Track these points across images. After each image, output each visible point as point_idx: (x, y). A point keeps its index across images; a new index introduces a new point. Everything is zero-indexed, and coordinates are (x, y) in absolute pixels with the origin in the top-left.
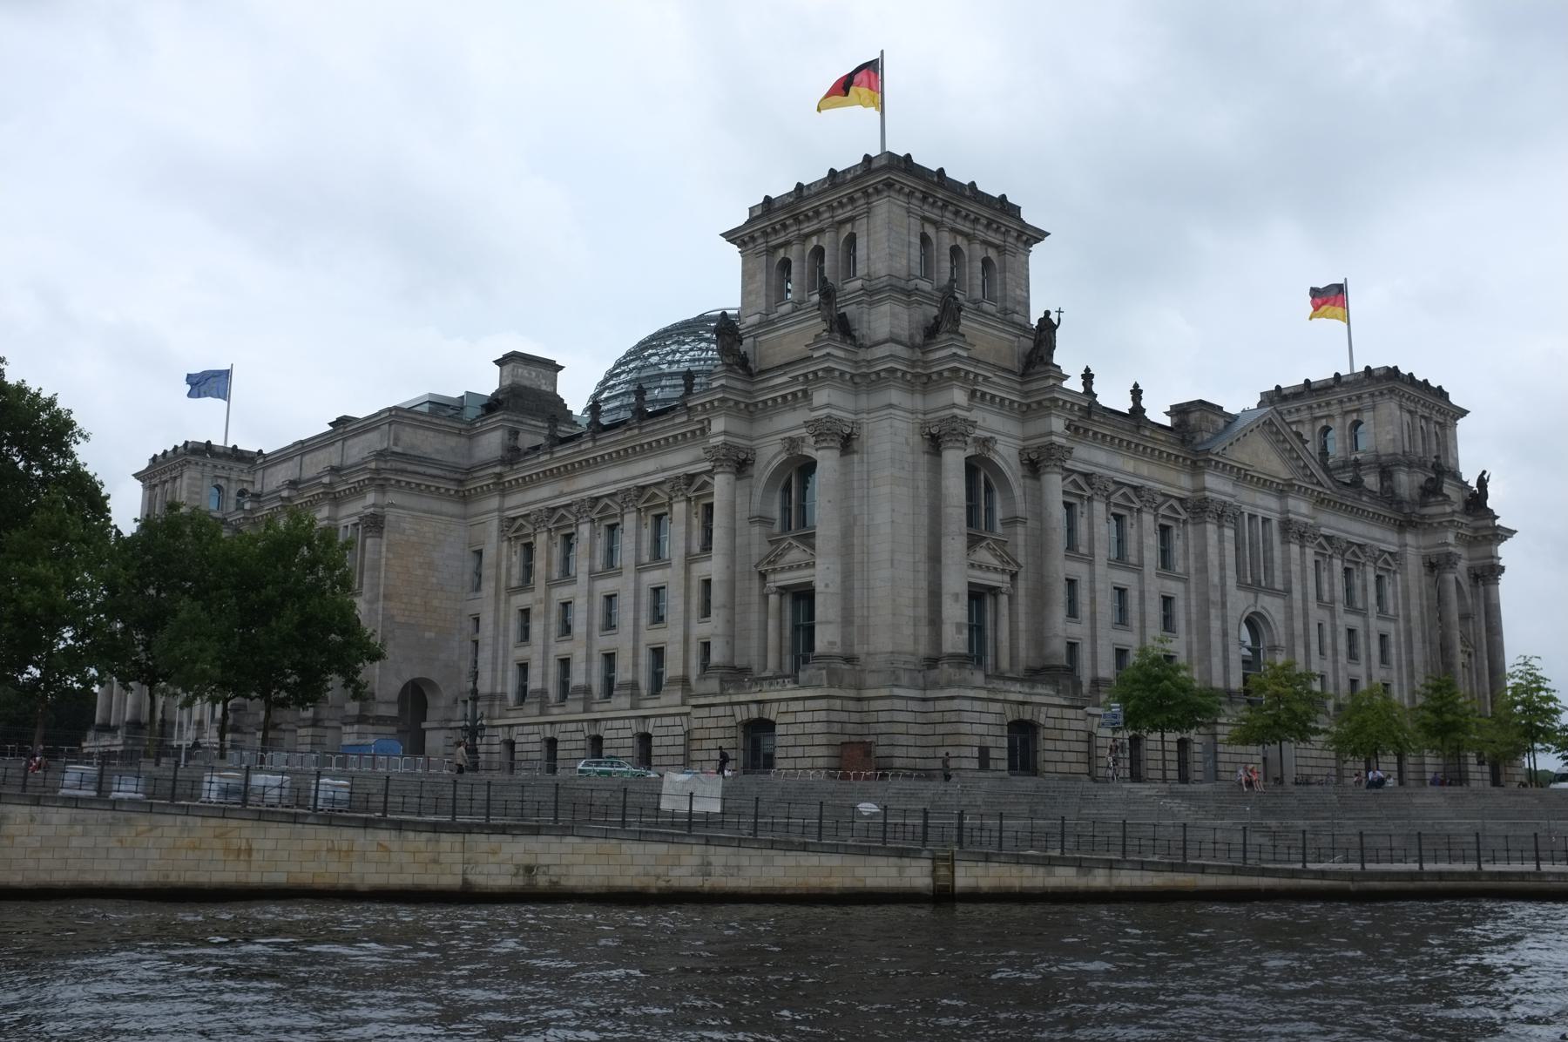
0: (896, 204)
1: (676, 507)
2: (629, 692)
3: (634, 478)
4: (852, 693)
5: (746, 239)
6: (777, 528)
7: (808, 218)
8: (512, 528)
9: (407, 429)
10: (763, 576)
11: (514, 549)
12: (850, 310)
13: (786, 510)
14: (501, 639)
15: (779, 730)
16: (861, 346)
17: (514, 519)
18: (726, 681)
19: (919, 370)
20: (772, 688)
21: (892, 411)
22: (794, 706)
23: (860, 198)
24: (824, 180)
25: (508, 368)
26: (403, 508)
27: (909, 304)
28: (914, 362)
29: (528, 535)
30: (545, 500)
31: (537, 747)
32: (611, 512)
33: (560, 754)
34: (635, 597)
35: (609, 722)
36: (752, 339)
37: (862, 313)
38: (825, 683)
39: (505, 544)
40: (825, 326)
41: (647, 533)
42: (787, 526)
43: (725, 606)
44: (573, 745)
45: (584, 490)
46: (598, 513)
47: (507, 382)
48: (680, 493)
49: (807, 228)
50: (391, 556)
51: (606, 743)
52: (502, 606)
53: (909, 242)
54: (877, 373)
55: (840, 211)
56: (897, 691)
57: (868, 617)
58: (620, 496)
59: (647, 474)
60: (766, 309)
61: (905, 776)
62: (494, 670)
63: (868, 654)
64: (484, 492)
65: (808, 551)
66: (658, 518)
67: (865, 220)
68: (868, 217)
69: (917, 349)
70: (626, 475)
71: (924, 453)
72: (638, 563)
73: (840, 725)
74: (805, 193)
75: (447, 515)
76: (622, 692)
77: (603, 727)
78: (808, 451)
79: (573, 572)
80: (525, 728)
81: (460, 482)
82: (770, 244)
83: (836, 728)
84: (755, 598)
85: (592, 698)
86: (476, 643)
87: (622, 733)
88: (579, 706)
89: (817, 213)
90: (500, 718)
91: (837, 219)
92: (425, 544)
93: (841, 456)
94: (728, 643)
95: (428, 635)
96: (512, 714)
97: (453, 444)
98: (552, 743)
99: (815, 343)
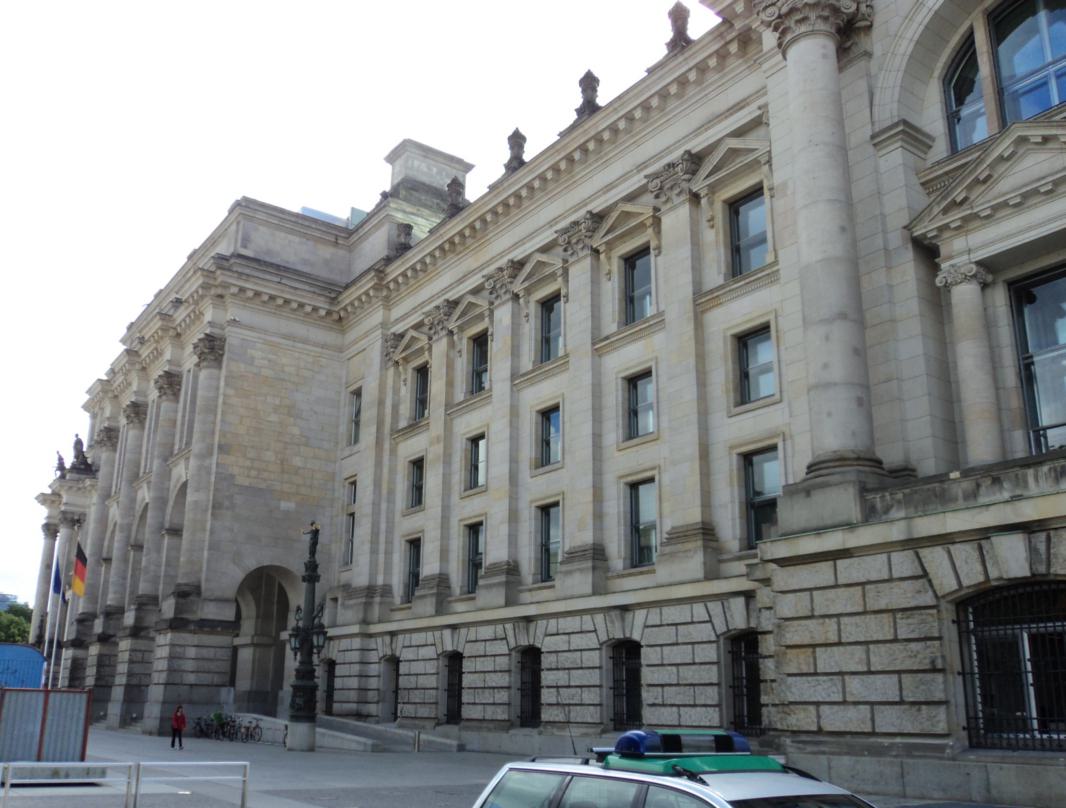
1: (667, 221)
2: (589, 564)
9: (261, 228)
10: (928, 252)
11: (403, 377)
14: (384, 506)
17: (402, 336)
26: (251, 328)
31: (431, 667)
33: (467, 680)
35: (553, 622)
39: (391, 371)
43: (843, 316)
44: (488, 664)
45: (501, 255)
47: (396, 181)
50: (231, 392)
51: (547, 661)
62: (374, 551)
64: (364, 301)
75: (316, 344)
76: (576, 566)
77: (540, 631)
79: (487, 385)
81: (333, 301)
85: (520, 583)
86: (352, 515)
87: (578, 641)
90: (380, 621)
92: (283, 380)
95: (284, 505)
96: (398, 615)
97: (328, 256)
98: (455, 659)
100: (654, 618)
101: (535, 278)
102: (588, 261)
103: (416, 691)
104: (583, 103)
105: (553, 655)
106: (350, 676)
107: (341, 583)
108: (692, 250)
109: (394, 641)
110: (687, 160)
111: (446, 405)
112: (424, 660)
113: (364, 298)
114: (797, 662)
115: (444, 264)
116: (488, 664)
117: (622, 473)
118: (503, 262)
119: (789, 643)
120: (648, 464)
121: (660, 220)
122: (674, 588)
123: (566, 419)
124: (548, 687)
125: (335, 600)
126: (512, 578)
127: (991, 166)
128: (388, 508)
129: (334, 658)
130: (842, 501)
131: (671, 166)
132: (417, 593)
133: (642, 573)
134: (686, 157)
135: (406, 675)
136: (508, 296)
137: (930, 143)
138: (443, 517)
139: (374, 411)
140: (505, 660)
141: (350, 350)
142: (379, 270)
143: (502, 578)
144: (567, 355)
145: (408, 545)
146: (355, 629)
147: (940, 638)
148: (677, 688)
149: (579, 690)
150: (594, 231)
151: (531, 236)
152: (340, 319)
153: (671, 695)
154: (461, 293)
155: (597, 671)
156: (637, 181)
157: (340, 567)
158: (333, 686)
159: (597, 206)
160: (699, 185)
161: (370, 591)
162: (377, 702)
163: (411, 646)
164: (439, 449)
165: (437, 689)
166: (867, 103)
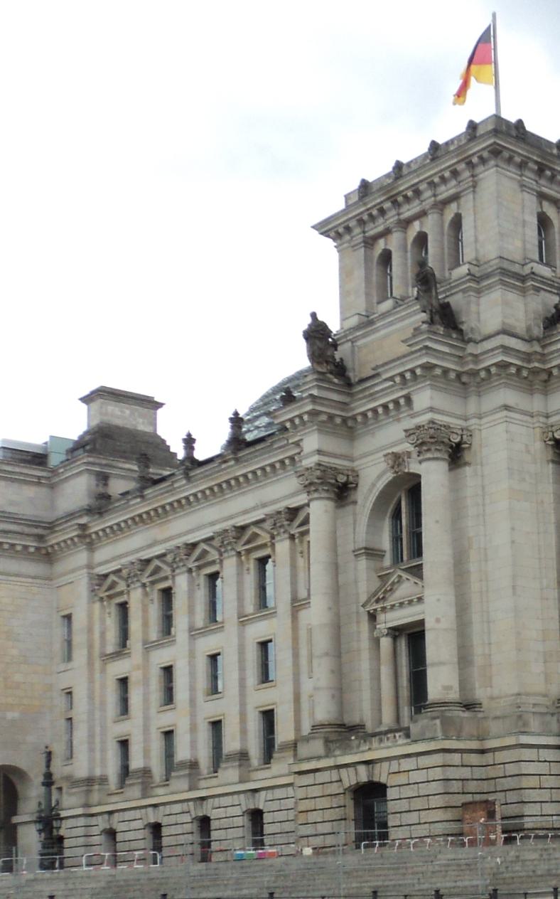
0: (503, 174)
1: (279, 547)
3: (231, 517)
4: (474, 745)
5: (341, 230)
6: (387, 561)
7: (407, 199)
8: (102, 584)
10: (372, 617)
11: (108, 610)
12: (456, 301)
13: (396, 539)
14: (97, 714)
15: (391, 793)
16: (470, 340)
17: (106, 576)
18: (332, 742)
19: (536, 364)
20: (382, 745)
21: (505, 413)
22: (407, 764)
23: (463, 170)
24: (425, 156)
25: (96, 405)
27: (523, 291)
28: (529, 354)
29: (121, 593)
30: (138, 551)
32: (210, 558)
36: (350, 344)
37: (469, 303)
38: (440, 734)
39: (97, 605)
40: (424, 316)
41: (250, 580)
42: (398, 558)
43: (327, 654)
45: (179, 535)
46: (196, 560)
47: (95, 422)
48: (282, 530)
49: (408, 211)
52: (97, 675)
53: (524, 221)
54: (487, 369)
55: (443, 188)
56: (525, 739)
57: (490, 655)
58: (217, 539)
59: (245, 512)
60: (367, 311)
61: (536, 837)
62: (91, 750)
63: (492, 698)
65: (420, 583)
66: (263, 561)
67: (471, 196)
68: (474, 192)
69: (535, 342)
70: (226, 514)
71: (548, 461)
72: (241, 615)
73: (460, 783)
74: (405, 171)
78: (414, 468)
82: (367, 234)
83: (456, 786)
84: (365, 643)
86: (70, 719)
89: (418, 193)
90: (99, 804)
91: (440, 198)
93: (450, 470)
94: (333, 696)
99: (414, 336)
102: (234, 559)
109: (111, 818)
118: (179, 542)
120: (270, 702)
127: (390, 584)
130: (317, 746)
132: (127, 782)
137: (383, 553)
146: (80, 811)
147: (345, 806)
151: (199, 528)
156: (258, 515)
160: (294, 531)
166: (352, 530)
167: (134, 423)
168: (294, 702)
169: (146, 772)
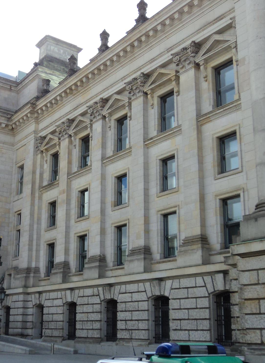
1: (182, 78)
2: (142, 256)
11: (45, 159)
14: (35, 226)
17: (45, 137)
31: (60, 310)
33: (79, 317)
34: (144, 169)
35: (123, 286)
39: (39, 156)
44: (89, 309)
45: (96, 95)
51: (120, 307)
62: (30, 250)
76: (135, 257)
77: (117, 291)
79: (89, 163)
80: (52, 294)
81: (9, 119)
85: (106, 266)
86: (19, 231)
87: (136, 297)
88: (95, 273)
90: (33, 286)
96: (43, 283)
97: (6, 96)
98: (72, 306)
100: (176, 285)
101: (114, 108)
102: (141, 99)
103: (52, 323)
104: (139, 17)
105: (124, 304)
106: (17, 315)
107: (13, 266)
108: (196, 93)
110: (193, 46)
111: (68, 174)
112: (56, 306)
113: (25, 118)
114: (251, 307)
115: (66, 100)
116: (89, 309)
117: (160, 209)
118: (97, 99)
119: (246, 297)
120: (173, 205)
121: (179, 77)
122: (186, 269)
123: (130, 181)
124: (121, 320)
125: (10, 275)
126: (102, 264)
128: (37, 227)
129: (9, 305)
131: (185, 49)
132: (52, 272)
133: (169, 261)
134: (193, 44)
135: (46, 314)
136: (100, 117)
138: (66, 232)
139: (30, 177)
140: (99, 306)
141: (18, 145)
142: (33, 103)
143: (97, 264)
144: (130, 148)
145: (48, 247)
146: (21, 290)
148: (188, 321)
149: (137, 322)
150: (145, 83)
151: (112, 86)
152: (13, 128)
153: (185, 325)
154: (76, 115)
155: (146, 312)
157: (12, 258)
158: (9, 320)
159: (146, 70)
160: (199, 59)
161: (28, 270)
162: (32, 328)
163: (49, 299)
164: (64, 196)
165: (63, 321)
167: (65, 57)
168: (200, 201)
169: (66, 265)
